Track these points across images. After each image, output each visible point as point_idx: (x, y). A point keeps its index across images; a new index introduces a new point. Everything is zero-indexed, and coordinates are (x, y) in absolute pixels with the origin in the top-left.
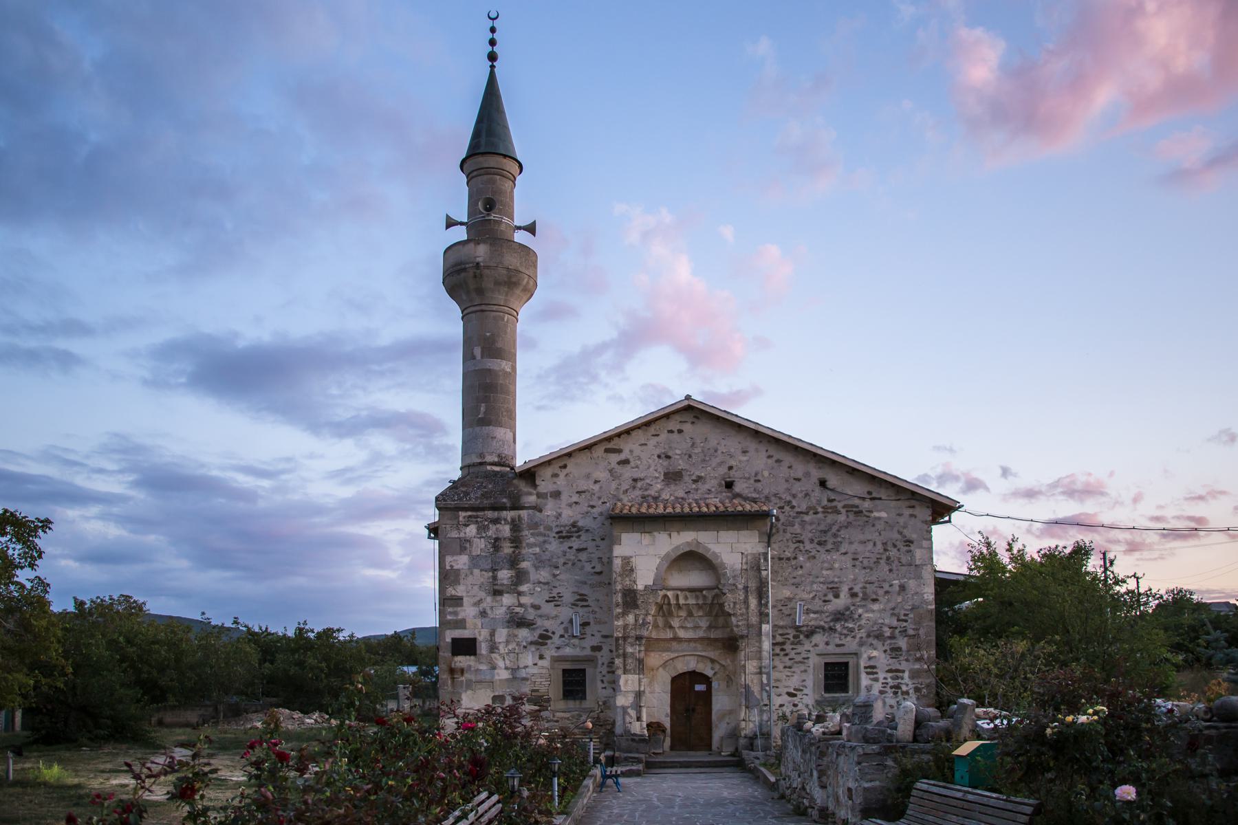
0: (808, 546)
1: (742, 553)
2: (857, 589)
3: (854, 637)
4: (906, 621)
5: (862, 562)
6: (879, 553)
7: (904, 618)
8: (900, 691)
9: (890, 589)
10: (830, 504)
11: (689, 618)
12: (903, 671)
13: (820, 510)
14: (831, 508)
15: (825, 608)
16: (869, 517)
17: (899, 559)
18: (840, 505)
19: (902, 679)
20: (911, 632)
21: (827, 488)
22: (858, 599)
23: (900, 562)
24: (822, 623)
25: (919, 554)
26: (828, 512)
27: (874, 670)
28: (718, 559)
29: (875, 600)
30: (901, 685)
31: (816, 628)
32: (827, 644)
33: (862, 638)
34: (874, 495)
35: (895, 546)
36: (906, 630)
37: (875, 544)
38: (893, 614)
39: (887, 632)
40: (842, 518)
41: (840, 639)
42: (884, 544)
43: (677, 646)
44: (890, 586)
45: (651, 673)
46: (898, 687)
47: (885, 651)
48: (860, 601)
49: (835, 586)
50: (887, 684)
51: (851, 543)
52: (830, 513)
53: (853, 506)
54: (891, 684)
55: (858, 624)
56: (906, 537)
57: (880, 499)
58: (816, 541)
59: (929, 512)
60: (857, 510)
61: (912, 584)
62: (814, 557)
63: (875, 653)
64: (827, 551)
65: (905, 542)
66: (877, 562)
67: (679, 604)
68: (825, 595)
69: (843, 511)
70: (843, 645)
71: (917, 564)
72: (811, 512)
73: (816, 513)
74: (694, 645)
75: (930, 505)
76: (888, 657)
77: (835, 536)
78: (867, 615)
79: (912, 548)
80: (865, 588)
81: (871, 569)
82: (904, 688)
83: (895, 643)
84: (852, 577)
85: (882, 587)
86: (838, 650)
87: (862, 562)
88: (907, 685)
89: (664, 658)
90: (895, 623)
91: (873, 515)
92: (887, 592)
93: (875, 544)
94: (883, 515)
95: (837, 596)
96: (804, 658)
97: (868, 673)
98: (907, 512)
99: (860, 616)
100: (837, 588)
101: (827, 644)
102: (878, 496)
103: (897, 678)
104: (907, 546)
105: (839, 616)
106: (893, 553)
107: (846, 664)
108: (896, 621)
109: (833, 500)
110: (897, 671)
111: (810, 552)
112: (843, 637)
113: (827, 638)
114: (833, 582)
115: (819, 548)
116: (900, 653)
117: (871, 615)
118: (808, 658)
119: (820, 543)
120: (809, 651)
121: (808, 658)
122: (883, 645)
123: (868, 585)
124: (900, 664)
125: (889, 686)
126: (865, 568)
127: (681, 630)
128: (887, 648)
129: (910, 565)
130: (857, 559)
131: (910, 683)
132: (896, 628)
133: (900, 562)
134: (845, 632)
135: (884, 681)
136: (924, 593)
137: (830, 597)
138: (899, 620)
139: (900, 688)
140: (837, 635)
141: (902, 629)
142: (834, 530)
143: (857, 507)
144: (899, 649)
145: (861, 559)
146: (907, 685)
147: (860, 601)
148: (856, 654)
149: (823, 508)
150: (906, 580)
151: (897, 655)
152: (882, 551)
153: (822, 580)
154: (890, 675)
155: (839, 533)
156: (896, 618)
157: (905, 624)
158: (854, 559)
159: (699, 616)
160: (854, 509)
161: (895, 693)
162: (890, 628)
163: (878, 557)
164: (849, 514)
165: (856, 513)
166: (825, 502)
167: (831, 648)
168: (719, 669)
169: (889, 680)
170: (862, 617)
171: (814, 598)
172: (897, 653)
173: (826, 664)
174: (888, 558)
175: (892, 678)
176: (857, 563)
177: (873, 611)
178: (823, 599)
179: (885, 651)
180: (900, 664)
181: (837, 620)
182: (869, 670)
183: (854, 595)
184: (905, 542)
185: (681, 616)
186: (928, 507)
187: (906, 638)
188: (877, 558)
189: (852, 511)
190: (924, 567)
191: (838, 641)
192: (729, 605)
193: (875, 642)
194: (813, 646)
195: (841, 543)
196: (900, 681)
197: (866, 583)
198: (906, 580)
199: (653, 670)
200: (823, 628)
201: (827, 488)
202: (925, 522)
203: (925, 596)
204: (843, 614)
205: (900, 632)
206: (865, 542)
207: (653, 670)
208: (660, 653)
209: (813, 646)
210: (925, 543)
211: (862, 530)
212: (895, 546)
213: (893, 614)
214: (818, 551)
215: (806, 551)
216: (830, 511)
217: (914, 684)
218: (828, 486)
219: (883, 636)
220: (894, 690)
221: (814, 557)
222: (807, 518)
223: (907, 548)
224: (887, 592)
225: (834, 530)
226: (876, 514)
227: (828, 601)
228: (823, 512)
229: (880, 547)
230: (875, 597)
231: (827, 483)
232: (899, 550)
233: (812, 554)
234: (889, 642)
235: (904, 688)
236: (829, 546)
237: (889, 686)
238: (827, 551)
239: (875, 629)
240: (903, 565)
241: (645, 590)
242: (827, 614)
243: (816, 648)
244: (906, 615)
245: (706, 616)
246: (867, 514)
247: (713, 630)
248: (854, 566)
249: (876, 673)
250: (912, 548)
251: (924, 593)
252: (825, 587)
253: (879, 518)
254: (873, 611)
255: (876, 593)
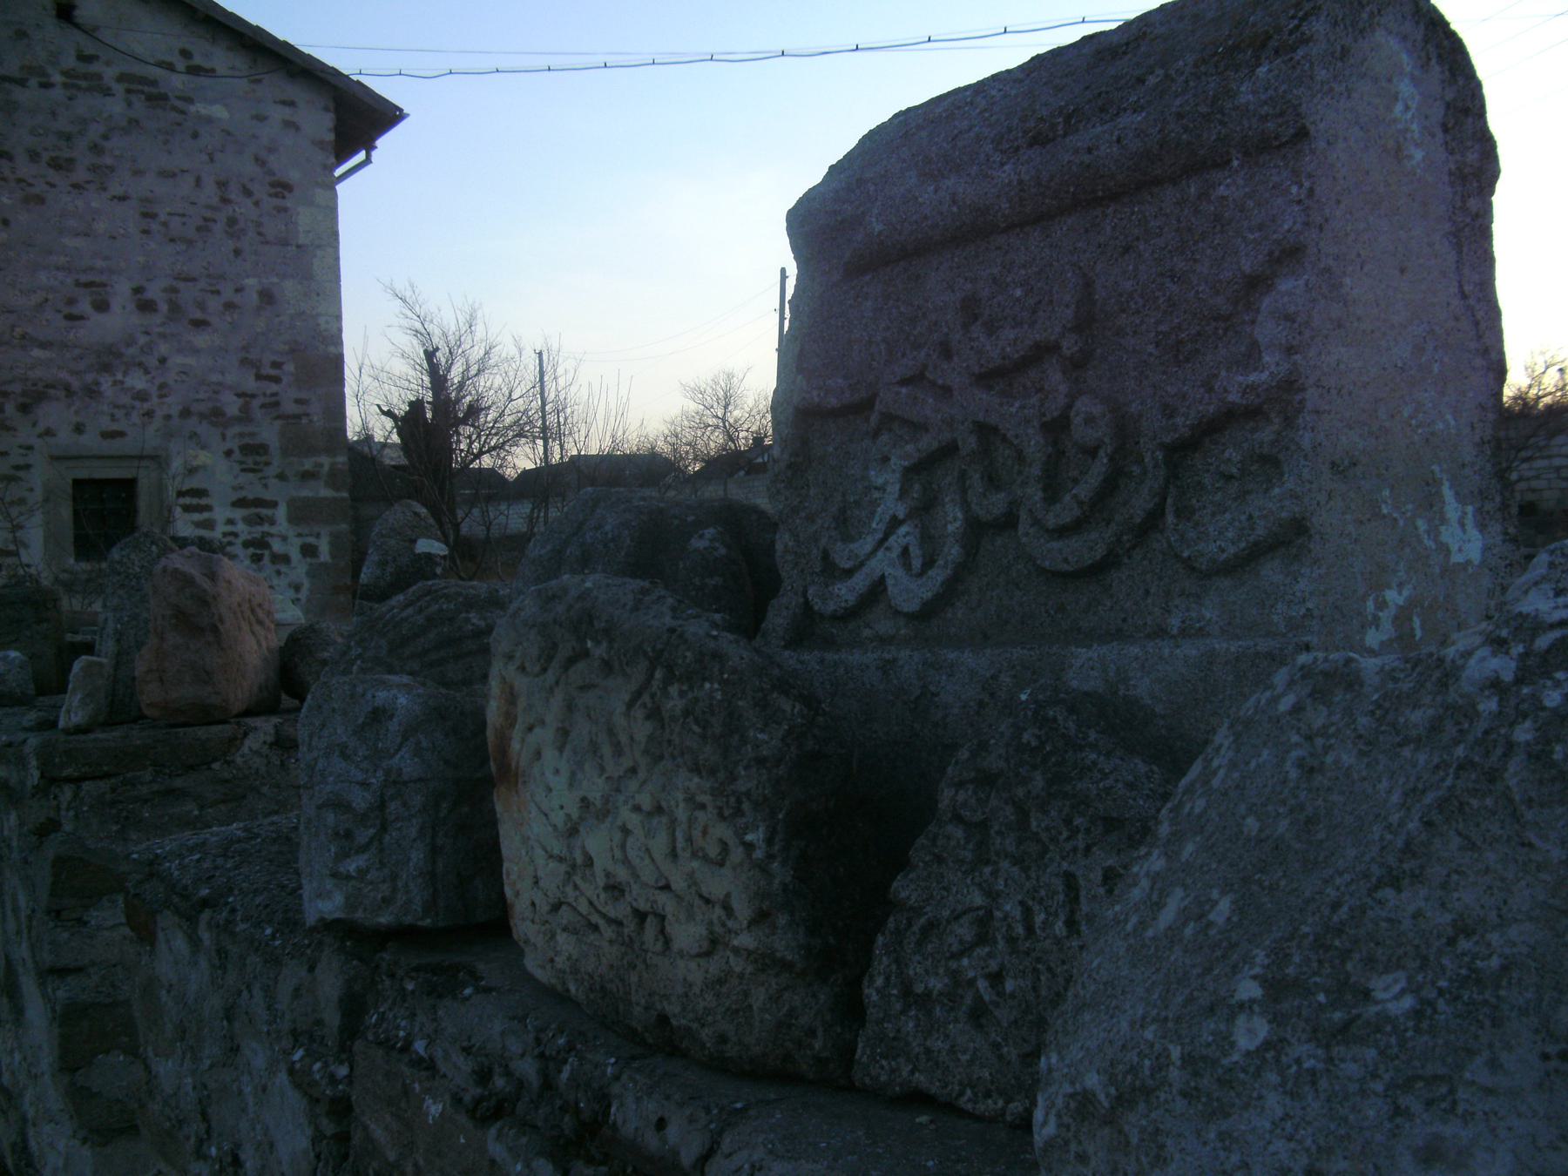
0: (25, 169)
2: (154, 292)
3: (149, 414)
4: (277, 380)
5: (165, 224)
6: (209, 207)
7: (273, 372)
8: (267, 553)
9: (237, 299)
10: (83, 68)
12: (274, 505)
13: (57, 78)
14: (85, 77)
15: (71, 336)
16: (183, 112)
17: (259, 224)
18: (109, 74)
19: (272, 522)
20: (289, 407)
21: (77, 26)
22: (157, 319)
23: (260, 234)
24: (64, 375)
25: (305, 218)
26: (79, 88)
27: (204, 501)
29: (199, 324)
30: (270, 540)
31: (47, 386)
32: (79, 429)
33: (168, 417)
34: (198, 60)
35: (248, 193)
36: (277, 404)
37: (198, 182)
38: (244, 362)
39: (232, 406)
40: (115, 107)
41: (113, 418)
42: (222, 185)
44: (238, 290)
46: (260, 544)
47: (229, 453)
48: (163, 324)
49: (97, 279)
50: (236, 535)
51: (138, 173)
52: (89, 89)
53: (143, 80)
54: (244, 537)
55: (158, 381)
56: (274, 174)
57: (210, 73)
58: (46, 156)
59: (328, 120)
60: (154, 90)
61: (289, 289)
62: (41, 200)
63: (203, 458)
64: (75, 186)
65: (273, 185)
66: (205, 228)
68: (71, 302)
69: (119, 88)
70: (121, 434)
71: (300, 242)
72: (33, 82)
73: (46, 86)
75: (331, 105)
76: (237, 467)
77: (96, 149)
78: (178, 360)
79: (288, 203)
80: (174, 290)
81: (190, 243)
82: (277, 546)
83: (252, 435)
84: (141, 259)
85: (218, 292)
86: (115, 446)
87: (165, 224)
88: (284, 539)
90: (251, 384)
91: (192, 109)
92: (229, 306)
93: (198, 182)
94: (219, 112)
95: (102, 306)
96: (17, 468)
97: (187, 509)
98: (278, 114)
99: (163, 361)
100: (105, 285)
101: (79, 429)
102: (207, 65)
103: (260, 520)
104: (276, 195)
105: (108, 358)
106: (244, 209)
107: (129, 485)
108: (253, 378)
109: (89, 59)
110: (259, 503)
111: (30, 185)
112: (119, 413)
113: (77, 412)
114: (92, 269)
115: (53, 176)
116: (264, 459)
117: (191, 361)
118: (28, 467)
119: (56, 164)
120: (30, 448)
121: (28, 467)
122: (224, 437)
123: (181, 285)
124: (265, 486)
125: (239, 541)
126: (172, 240)
128: (233, 444)
129: (285, 243)
130: (153, 216)
131: (291, 534)
132: (253, 396)
133: (260, 234)
134: (126, 400)
135: (229, 528)
136: (318, 315)
137: (85, 306)
138: (259, 377)
139: (267, 546)
140: (105, 408)
141: (268, 400)
142: (94, 132)
143: (154, 83)
144: (261, 449)
145: (163, 217)
146: (284, 539)
147: (163, 324)
148: (152, 458)
149: (65, 73)
150: (275, 280)
151: (256, 463)
152: (215, 201)
153: (62, 260)
154: (239, 514)
155: (108, 145)
156: (254, 371)
157: (274, 388)
158: (145, 215)
160: (146, 89)
161: (257, 559)
162: (239, 395)
163: (208, 214)
164: (134, 98)
165: (150, 98)
166: (70, 62)
167: (90, 441)
169: (241, 527)
170: (170, 363)
171: (41, 306)
172: (258, 459)
173: (77, 483)
174: (232, 222)
175: (248, 521)
176: (155, 227)
177: (196, 351)
178: (66, 310)
179: (229, 453)
180: (265, 486)
181: (106, 368)
182: (187, 500)
183: (146, 306)
184: (273, 185)
186: (326, 109)
187: (278, 423)
188: (205, 219)
189: (142, 92)
190: (319, 253)
191: (106, 424)
193: (203, 429)
194: (40, 436)
195: (112, 169)
196: (266, 528)
197: (175, 279)
198: (275, 280)
200: (68, 389)
201: (77, 26)
202: (320, 144)
203: (322, 321)
204: (119, 355)
205: (263, 406)
206: (174, 175)
209: (40, 436)
210: (320, 195)
211: (166, 142)
212: (248, 193)
213: (244, 362)
214: (53, 186)
215: (20, 181)
216: (84, 84)
217: (300, 535)
218: (79, 21)
219: (223, 414)
220: (251, 550)
221: (41, 200)
222: (20, 94)
223: (278, 202)
224: (229, 306)
225: (94, 132)
226: (200, 108)
227: (81, 318)
228: (66, 86)
229: (210, 193)
230: (198, 315)
231: (77, 13)
232: (257, 204)
233: (36, 190)
234: (237, 429)
235: (277, 546)
236: (81, 175)
237: (239, 541)
238: (75, 186)
239: (201, 396)
240: (267, 243)
242: (77, 352)
243: (48, 439)
244: (276, 365)
246: (179, 104)
248: (146, 232)
249: (208, 508)
250: (288, 203)
251: (318, 315)
252: (69, 281)
253: (209, 120)
254: (196, 351)
255: (202, 306)
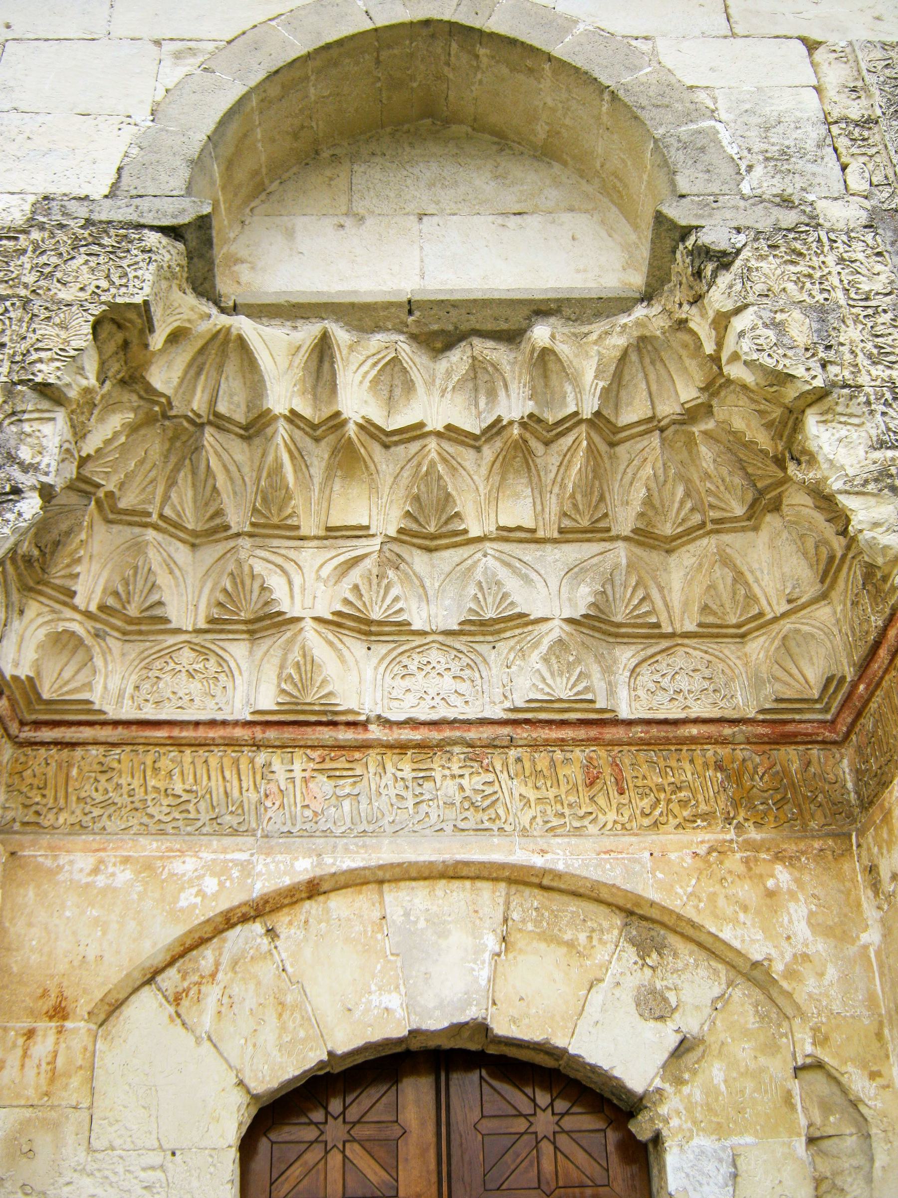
1: (811, 46)
11: (419, 561)
28: (633, 69)
43: (323, 785)
45: (42, 1047)
67: (336, 422)
74: (473, 782)
89: (187, 899)
127: (355, 647)
159: (506, 535)
168: (719, 1003)
185: (360, 532)
192: (779, 327)
199: (59, 1012)
207: (59, 1012)
208: (150, 847)
241: (32, 223)
245: (566, 536)
247: (626, 656)
